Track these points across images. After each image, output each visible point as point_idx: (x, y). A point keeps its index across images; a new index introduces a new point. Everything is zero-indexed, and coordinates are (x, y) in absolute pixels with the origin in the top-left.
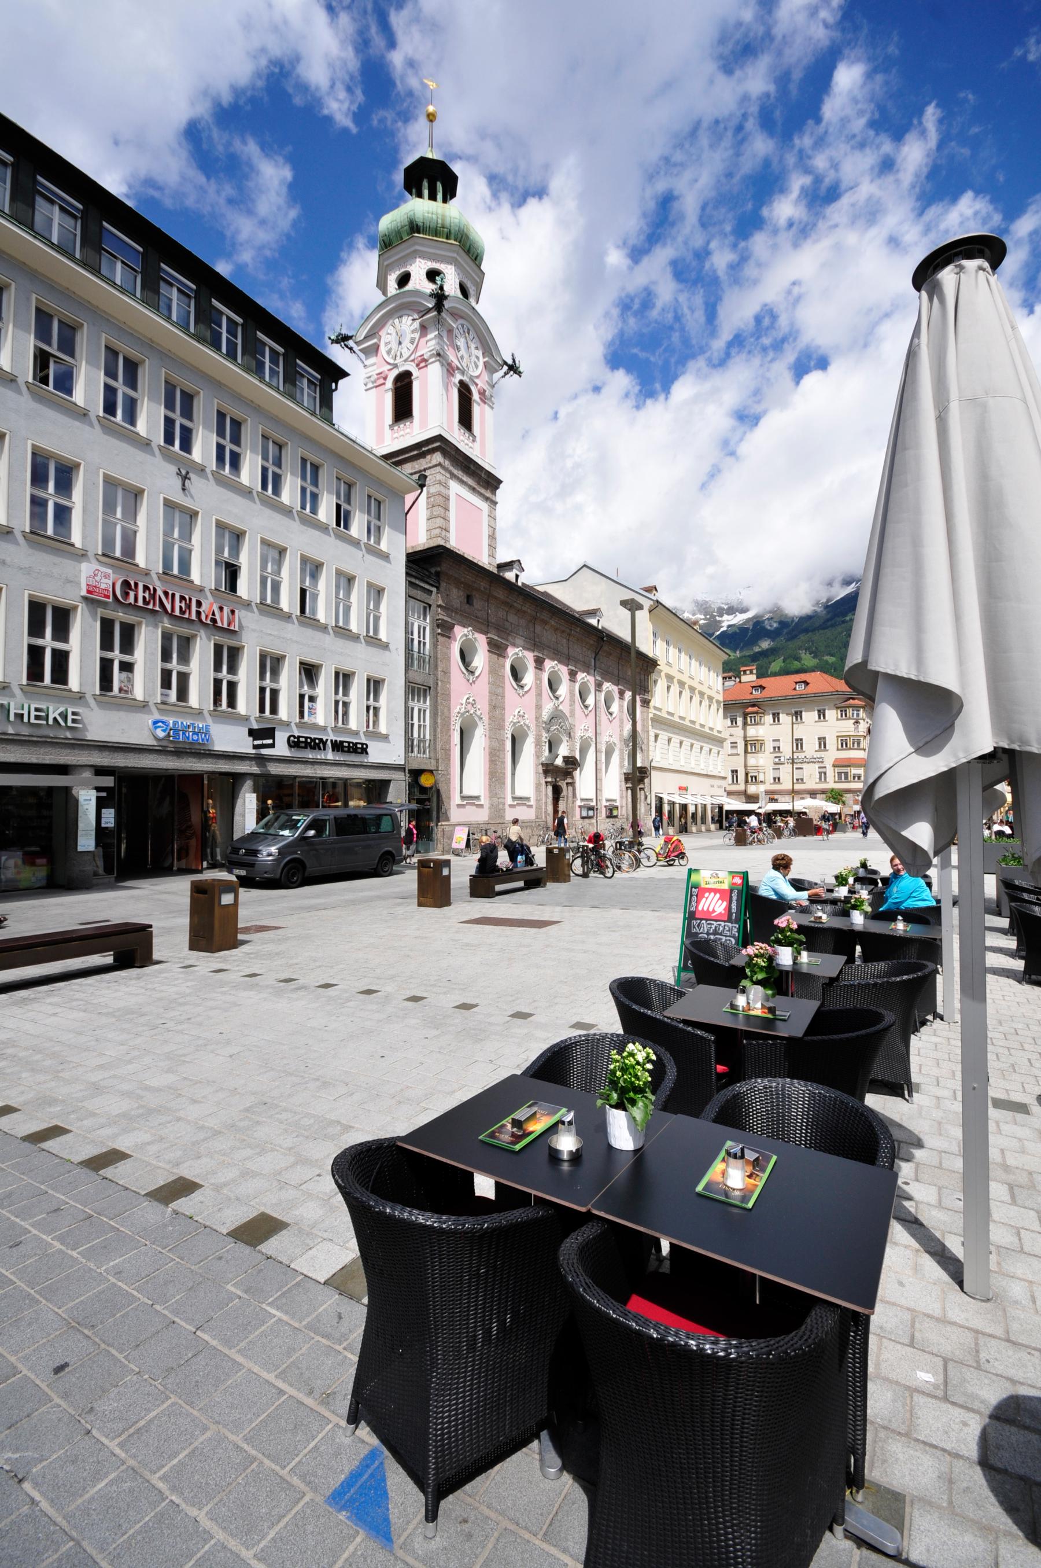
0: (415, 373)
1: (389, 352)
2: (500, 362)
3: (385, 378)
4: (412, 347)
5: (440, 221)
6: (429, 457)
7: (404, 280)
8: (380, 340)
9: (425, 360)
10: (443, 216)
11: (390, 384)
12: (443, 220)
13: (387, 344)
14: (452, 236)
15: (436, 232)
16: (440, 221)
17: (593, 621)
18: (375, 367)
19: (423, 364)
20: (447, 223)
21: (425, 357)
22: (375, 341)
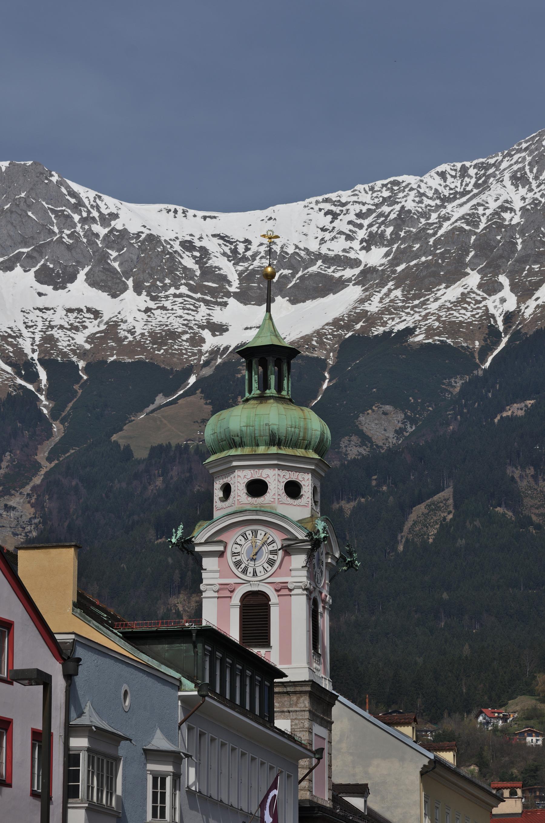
0: (274, 598)
1: (238, 564)
2: (337, 555)
3: (232, 592)
4: (271, 570)
5: (302, 434)
6: (294, 698)
7: (257, 488)
8: (225, 547)
9: (291, 590)
10: (306, 429)
11: (236, 599)
12: (305, 433)
13: (234, 554)
14: (311, 448)
15: (295, 445)
16: (302, 434)
17: (357, 802)
18: (217, 575)
19: (283, 592)
20: (308, 437)
21: (290, 586)
22: (221, 548)
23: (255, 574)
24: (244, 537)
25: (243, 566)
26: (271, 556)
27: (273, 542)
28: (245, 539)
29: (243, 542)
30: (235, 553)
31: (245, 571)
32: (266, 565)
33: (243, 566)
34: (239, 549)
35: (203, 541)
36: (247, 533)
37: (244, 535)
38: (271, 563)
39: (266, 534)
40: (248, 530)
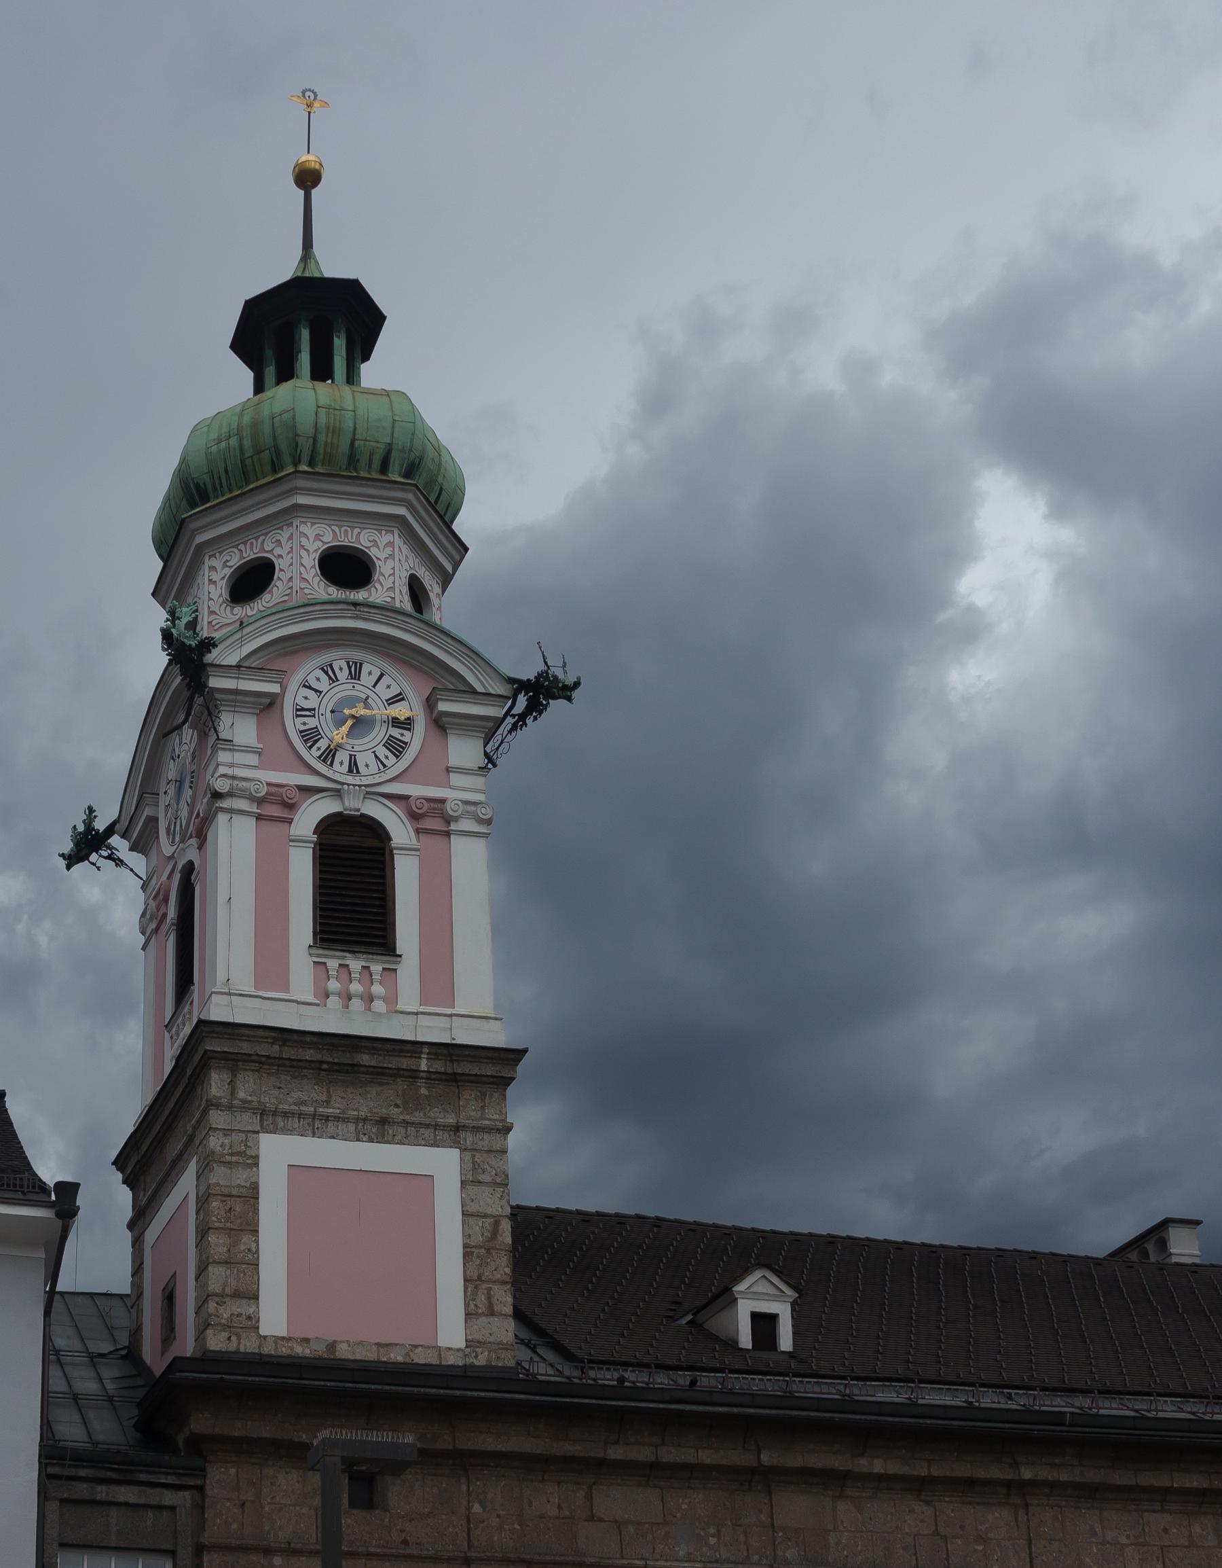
1: (311, 737)
9: (448, 820)
13: (299, 711)
22: (274, 688)
23: (353, 767)
24: (326, 673)
25: (323, 744)
26: (395, 732)
27: (398, 698)
28: (330, 678)
29: (324, 684)
30: (303, 709)
31: (328, 756)
32: (382, 752)
33: (323, 744)
34: (313, 701)
35: (232, 660)
36: (336, 666)
37: (328, 670)
38: (397, 748)
39: (382, 675)
40: (339, 659)
